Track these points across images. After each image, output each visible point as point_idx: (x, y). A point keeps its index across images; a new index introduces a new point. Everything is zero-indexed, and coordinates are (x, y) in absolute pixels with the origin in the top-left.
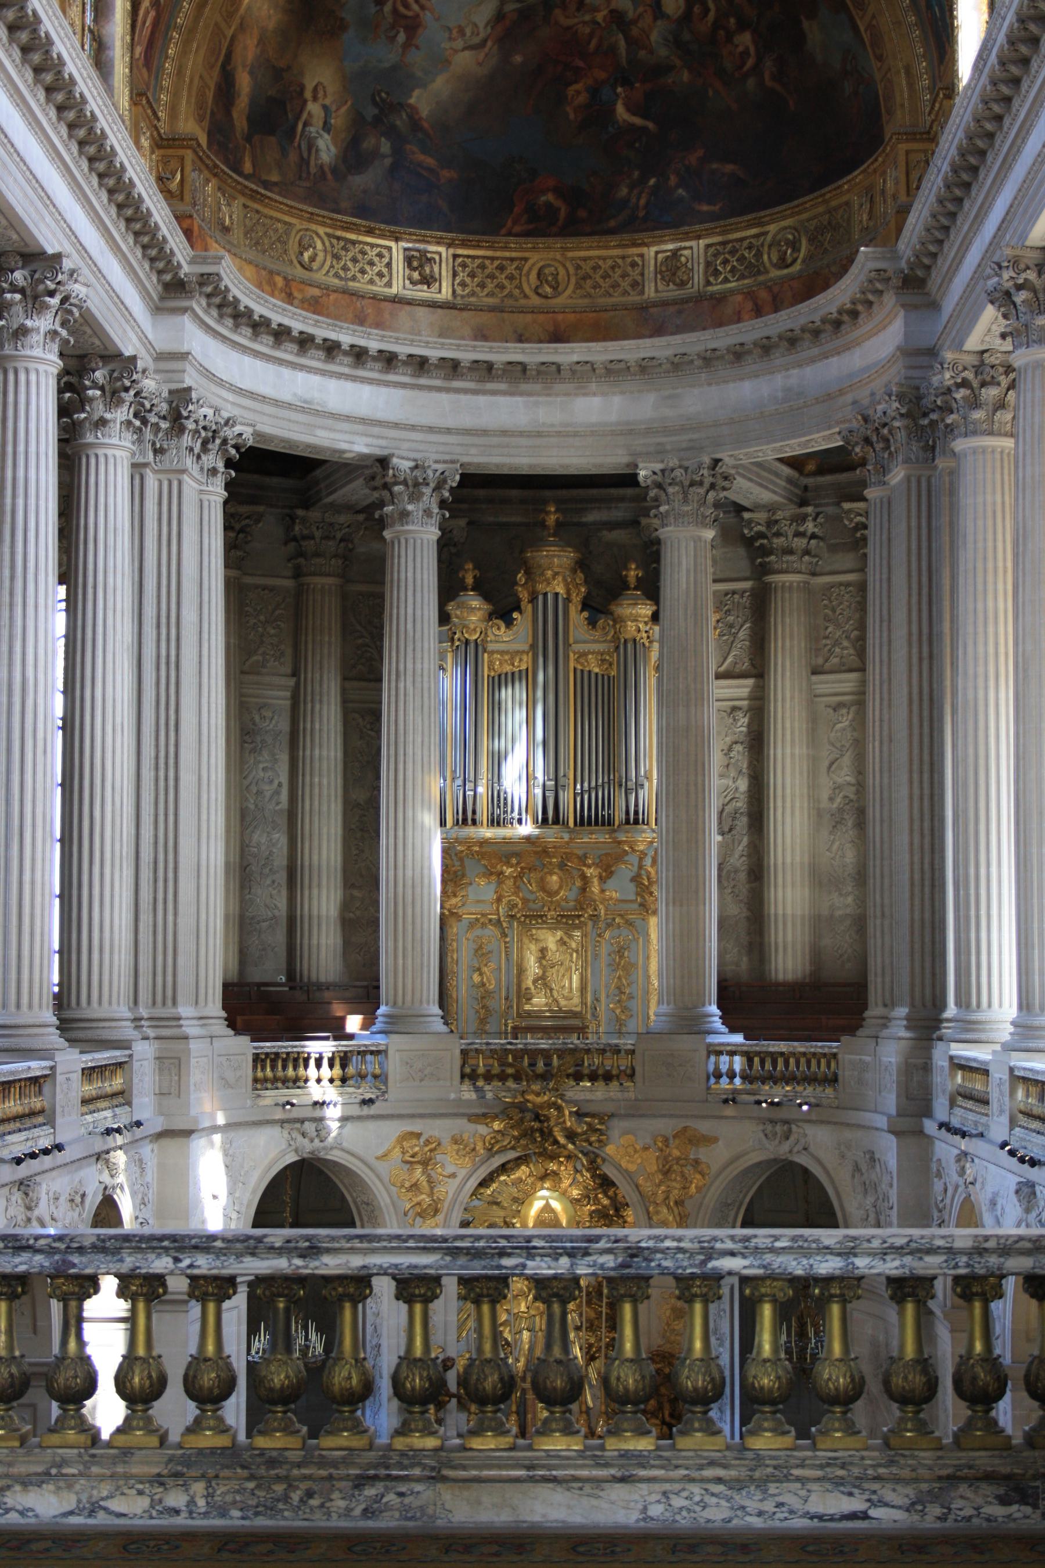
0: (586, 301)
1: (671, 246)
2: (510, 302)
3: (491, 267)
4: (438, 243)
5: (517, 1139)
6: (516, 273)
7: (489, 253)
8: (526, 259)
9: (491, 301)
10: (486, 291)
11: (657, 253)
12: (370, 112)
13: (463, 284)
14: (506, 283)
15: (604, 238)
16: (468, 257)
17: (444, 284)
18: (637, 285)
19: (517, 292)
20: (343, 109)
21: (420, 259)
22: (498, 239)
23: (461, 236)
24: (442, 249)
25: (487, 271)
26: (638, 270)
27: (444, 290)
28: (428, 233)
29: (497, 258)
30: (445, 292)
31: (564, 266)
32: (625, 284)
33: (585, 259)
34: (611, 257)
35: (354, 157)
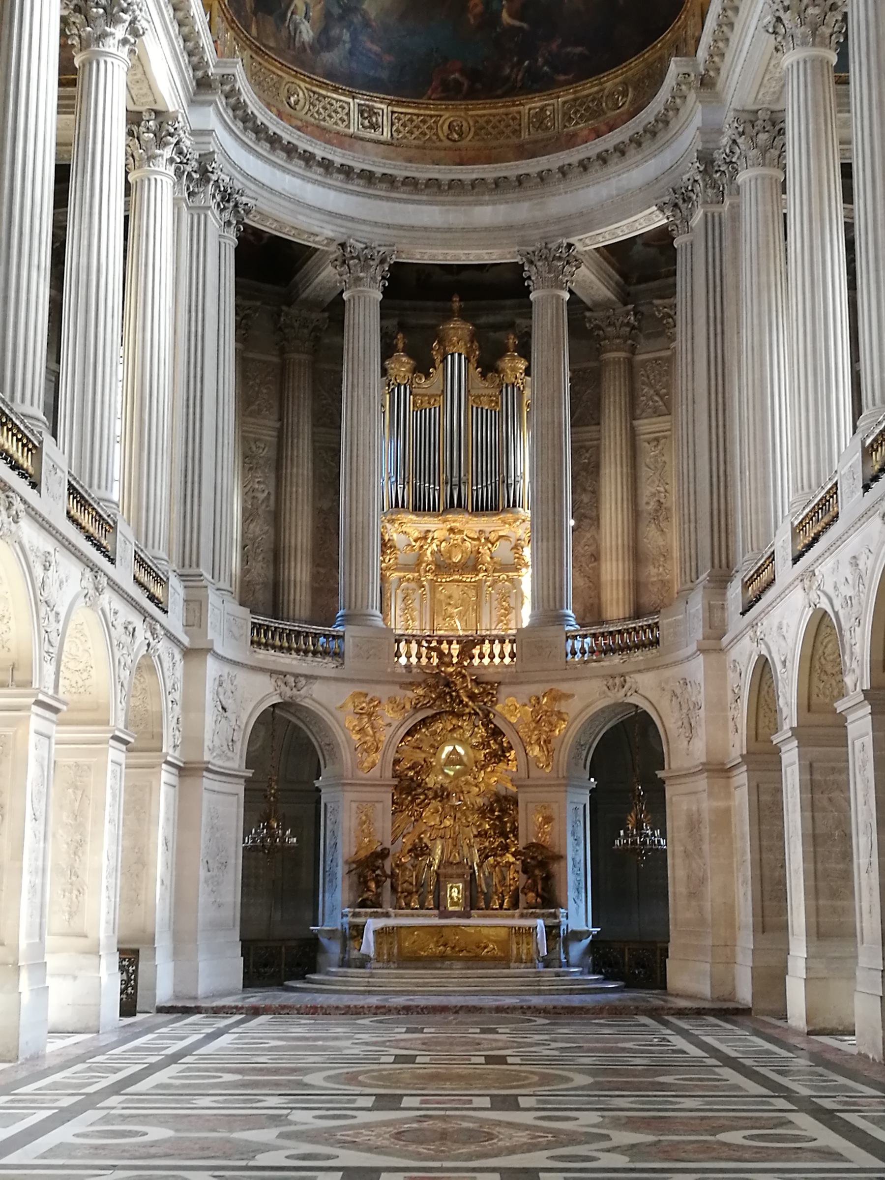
0: (481, 144)
1: (539, 104)
2: (428, 144)
3: (417, 120)
4: (381, 102)
5: (435, 700)
6: (434, 126)
7: (416, 111)
8: (441, 116)
9: (416, 142)
10: (413, 136)
11: (530, 109)
12: (336, 11)
13: (398, 131)
14: (427, 131)
15: (494, 101)
16: (402, 113)
17: (385, 130)
18: (517, 132)
19: (435, 137)
20: (319, 7)
21: (369, 112)
22: (421, 101)
23: (396, 98)
24: (384, 106)
25: (414, 123)
26: (517, 122)
27: (385, 133)
28: (375, 95)
29: (421, 115)
30: (386, 136)
31: (467, 121)
32: (508, 131)
33: (481, 116)
34: (498, 114)
35: (324, 41)
